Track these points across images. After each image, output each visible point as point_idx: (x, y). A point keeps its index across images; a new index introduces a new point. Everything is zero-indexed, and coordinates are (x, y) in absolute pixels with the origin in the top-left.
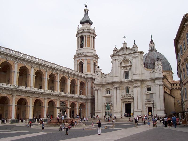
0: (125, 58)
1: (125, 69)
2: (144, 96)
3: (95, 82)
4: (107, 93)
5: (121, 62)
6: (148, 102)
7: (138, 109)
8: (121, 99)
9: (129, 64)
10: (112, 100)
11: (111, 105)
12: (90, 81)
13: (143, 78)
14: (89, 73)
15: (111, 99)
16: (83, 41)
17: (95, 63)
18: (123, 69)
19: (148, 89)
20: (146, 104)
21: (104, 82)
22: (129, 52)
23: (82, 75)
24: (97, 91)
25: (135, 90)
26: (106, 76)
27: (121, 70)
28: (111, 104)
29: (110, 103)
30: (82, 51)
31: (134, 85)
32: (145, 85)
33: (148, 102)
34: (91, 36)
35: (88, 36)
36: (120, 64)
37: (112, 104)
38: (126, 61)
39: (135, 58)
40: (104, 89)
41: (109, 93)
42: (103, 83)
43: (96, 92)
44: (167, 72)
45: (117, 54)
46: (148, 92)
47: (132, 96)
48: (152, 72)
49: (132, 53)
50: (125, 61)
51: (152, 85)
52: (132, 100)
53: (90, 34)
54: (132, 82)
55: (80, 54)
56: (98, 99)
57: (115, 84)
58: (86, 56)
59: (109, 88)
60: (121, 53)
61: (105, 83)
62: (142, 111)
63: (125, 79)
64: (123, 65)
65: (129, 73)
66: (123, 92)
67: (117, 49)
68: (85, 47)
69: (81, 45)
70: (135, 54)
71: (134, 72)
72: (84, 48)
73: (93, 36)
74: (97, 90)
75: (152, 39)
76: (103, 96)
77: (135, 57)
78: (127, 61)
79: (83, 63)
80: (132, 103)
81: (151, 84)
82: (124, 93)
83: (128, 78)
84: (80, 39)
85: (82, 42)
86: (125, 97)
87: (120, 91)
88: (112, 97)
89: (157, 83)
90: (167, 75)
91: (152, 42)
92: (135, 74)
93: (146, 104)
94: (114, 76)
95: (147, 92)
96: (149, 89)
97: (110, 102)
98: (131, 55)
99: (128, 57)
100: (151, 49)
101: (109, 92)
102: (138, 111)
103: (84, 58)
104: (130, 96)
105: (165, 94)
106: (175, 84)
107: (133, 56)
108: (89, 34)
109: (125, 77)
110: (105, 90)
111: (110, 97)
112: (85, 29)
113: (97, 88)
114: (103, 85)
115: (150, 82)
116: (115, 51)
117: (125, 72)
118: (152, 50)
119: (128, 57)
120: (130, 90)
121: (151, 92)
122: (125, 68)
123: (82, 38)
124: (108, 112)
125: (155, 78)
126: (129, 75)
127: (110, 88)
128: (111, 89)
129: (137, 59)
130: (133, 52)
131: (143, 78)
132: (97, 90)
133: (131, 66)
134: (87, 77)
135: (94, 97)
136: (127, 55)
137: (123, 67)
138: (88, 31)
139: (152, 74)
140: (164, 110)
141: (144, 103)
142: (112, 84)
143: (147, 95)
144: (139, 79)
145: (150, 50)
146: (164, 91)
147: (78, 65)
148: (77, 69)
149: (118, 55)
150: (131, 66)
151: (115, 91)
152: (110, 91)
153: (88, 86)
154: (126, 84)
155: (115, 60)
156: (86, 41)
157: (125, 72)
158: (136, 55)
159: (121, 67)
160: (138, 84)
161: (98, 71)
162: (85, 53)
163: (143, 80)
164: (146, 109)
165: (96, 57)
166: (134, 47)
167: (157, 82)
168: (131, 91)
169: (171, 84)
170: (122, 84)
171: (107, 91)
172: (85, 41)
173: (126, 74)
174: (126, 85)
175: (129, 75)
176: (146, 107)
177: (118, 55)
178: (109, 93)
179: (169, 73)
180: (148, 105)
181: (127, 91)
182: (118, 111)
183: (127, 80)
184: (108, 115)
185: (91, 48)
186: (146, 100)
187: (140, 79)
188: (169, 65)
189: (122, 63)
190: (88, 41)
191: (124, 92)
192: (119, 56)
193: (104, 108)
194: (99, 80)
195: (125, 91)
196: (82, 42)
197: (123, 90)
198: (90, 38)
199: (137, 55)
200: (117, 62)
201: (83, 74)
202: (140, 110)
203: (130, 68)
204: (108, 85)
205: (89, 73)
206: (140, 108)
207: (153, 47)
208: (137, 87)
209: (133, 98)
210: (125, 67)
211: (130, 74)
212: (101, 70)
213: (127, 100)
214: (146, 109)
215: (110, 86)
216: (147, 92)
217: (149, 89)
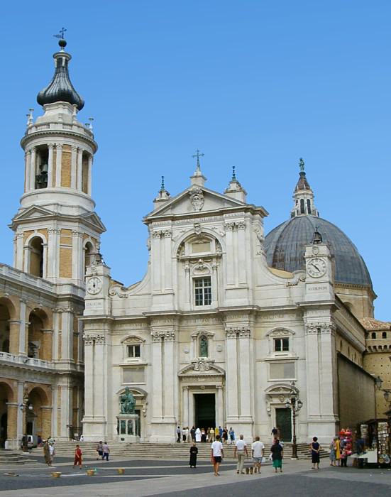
0: (197, 229)
1: (196, 269)
2: (264, 369)
3: (86, 313)
4: (131, 354)
5: (183, 244)
6: (278, 389)
7: (239, 414)
8: (180, 378)
9: (212, 250)
10: (147, 379)
11: (143, 398)
12: (69, 310)
13: (261, 303)
14: (65, 280)
15: (144, 376)
16: (47, 163)
17: (88, 246)
18: (187, 266)
19: (277, 342)
20: (270, 396)
21: (117, 313)
22: (210, 206)
23: (38, 284)
24: (94, 345)
25: (231, 343)
26: (127, 293)
27: (182, 273)
28: (143, 395)
29: (139, 389)
30: (43, 199)
31: (228, 325)
32: (269, 326)
33: (278, 389)
34: (78, 149)
35: (64, 146)
36: (180, 248)
37: (146, 394)
38: (201, 238)
39: (235, 230)
40: (117, 340)
41: (138, 355)
42: (114, 317)
43: (88, 349)
44: (355, 292)
45: (169, 213)
46: (278, 353)
47: (221, 366)
48: (293, 281)
49: (221, 213)
50: (195, 240)
51: (293, 329)
52: (218, 383)
53: (72, 140)
54: (221, 316)
55: (35, 210)
56: (93, 375)
57: (159, 323)
58: (58, 218)
59: (135, 337)
60: (181, 210)
61: (121, 317)
62: (253, 423)
63: (197, 304)
64: (189, 252)
65: (210, 285)
66: (186, 353)
67: (168, 194)
68: (54, 186)
69: (37, 178)
70: (233, 214)
71: (230, 279)
72: (49, 188)
73: (84, 147)
74: (94, 341)
75: (303, 174)
76: (115, 366)
77: (235, 227)
78: (204, 241)
79: (45, 242)
80: (220, 391)
81: (289, 323)
82: (192, 354)
83: (208, 302)
84: (36, 157)
85: (41, 167)
86: (193, 369)
87: (174, 347)
88: (147, 369)
89: (313, 321)
90: (352, 302)
91: (303, 183)
92: (233, 287)
93: (270, 396)
94: (156, 293)
95: (274, 355)
96: (282, 344)
97: (141, 387)
98: (220, 220)
99: (207, 226)
100: (299, 209)
101: (135, 351)
102: (241, 420)
103: (50, 225)
104: (211, 368)
105: (342, 363)
106: (381, 333)
107: (227, 221)
108: (70, 141)
109: (197, 298)
110: (122, 342)
111: (141, 368)
112: (55, 123)
113: (93, 334)
114: (113, 323)
115: (287, 317)
116: (162, 203)
118: (303, 211)
119: (207, 226)
120: (212, 346)
121: (289, 354)
122: (197, 266)
123: (43, 152)
124: (130, 422)
125: (305, 303)
126: (210, 291)
127: (139, 335)
128: (144, 341)
129: (241, 231)
130: (227, 207)
131: (261, 304)
132: (94, 341)
133: (219, 257)
134: (58, 295)
135: (83, 367)
136: (203, 219)
137: (191, 260)
138: (68, 129)
139: (294, 289)
140: (333, 419)
141: (262, 394)
142: (148, 320)
143: (273, 362)
144: (246, 307)
145: (294, 213)
146: (335, 355)
147: (27, 251)
148: (23, 263)
149: (173, 219)
150: (219, 257)
151: (157, 348)
152: (141, 347)
153: (60, 328)
154: (199, 322)
155: (162, 235)
156: (59, 166)
158: (239, 218)
159: (183, 261)
160: (243, 323)
161: (97, 274)
162: (51, 208)
163: (260, 308)
164: (270, 416)
165: (95, 223)
166: (232, 192)
167: (312, 318)
168: (215, 349)
169: (366, 333)
170: (184, 323)
171: (130, 348)
172: (54, 164)
173: (201, 285)
174: (199, 327)
175: (210, 289)
176: (269, 410)
177: (173, 219)
178: (138, 355)
179: (359, 292)
180: (276, 401)
181: (201, 347)
182: (166, 421)
183: (204, 307)
184: (129, 433)
185: (75, 191)
186: (270, 384)
187: (250, 306)
188: (360, 266)
189: (186, 245)
190: (66, 166)
191: (191, 354)
192: (176, 222)
193: (117, 408)
194: (99, 304)
195: (194, 347)
196: (44, 170)
197: (187, 345)
198: (74, 153)
199: (242, 220)
200: (167, 240)
201: (44, 281)
202: (249, 420)
203: (214, 264)
204: (134, 326)
205: (65, 280)
206: (246, 412)
207: (306, 201)
210: (196, 259)
211: (213, 288)
212: (110, 268)
213: (201, 382)
214: (270, 416)
215: (139, 327)
216: (274, 355)
217: (282, 344)
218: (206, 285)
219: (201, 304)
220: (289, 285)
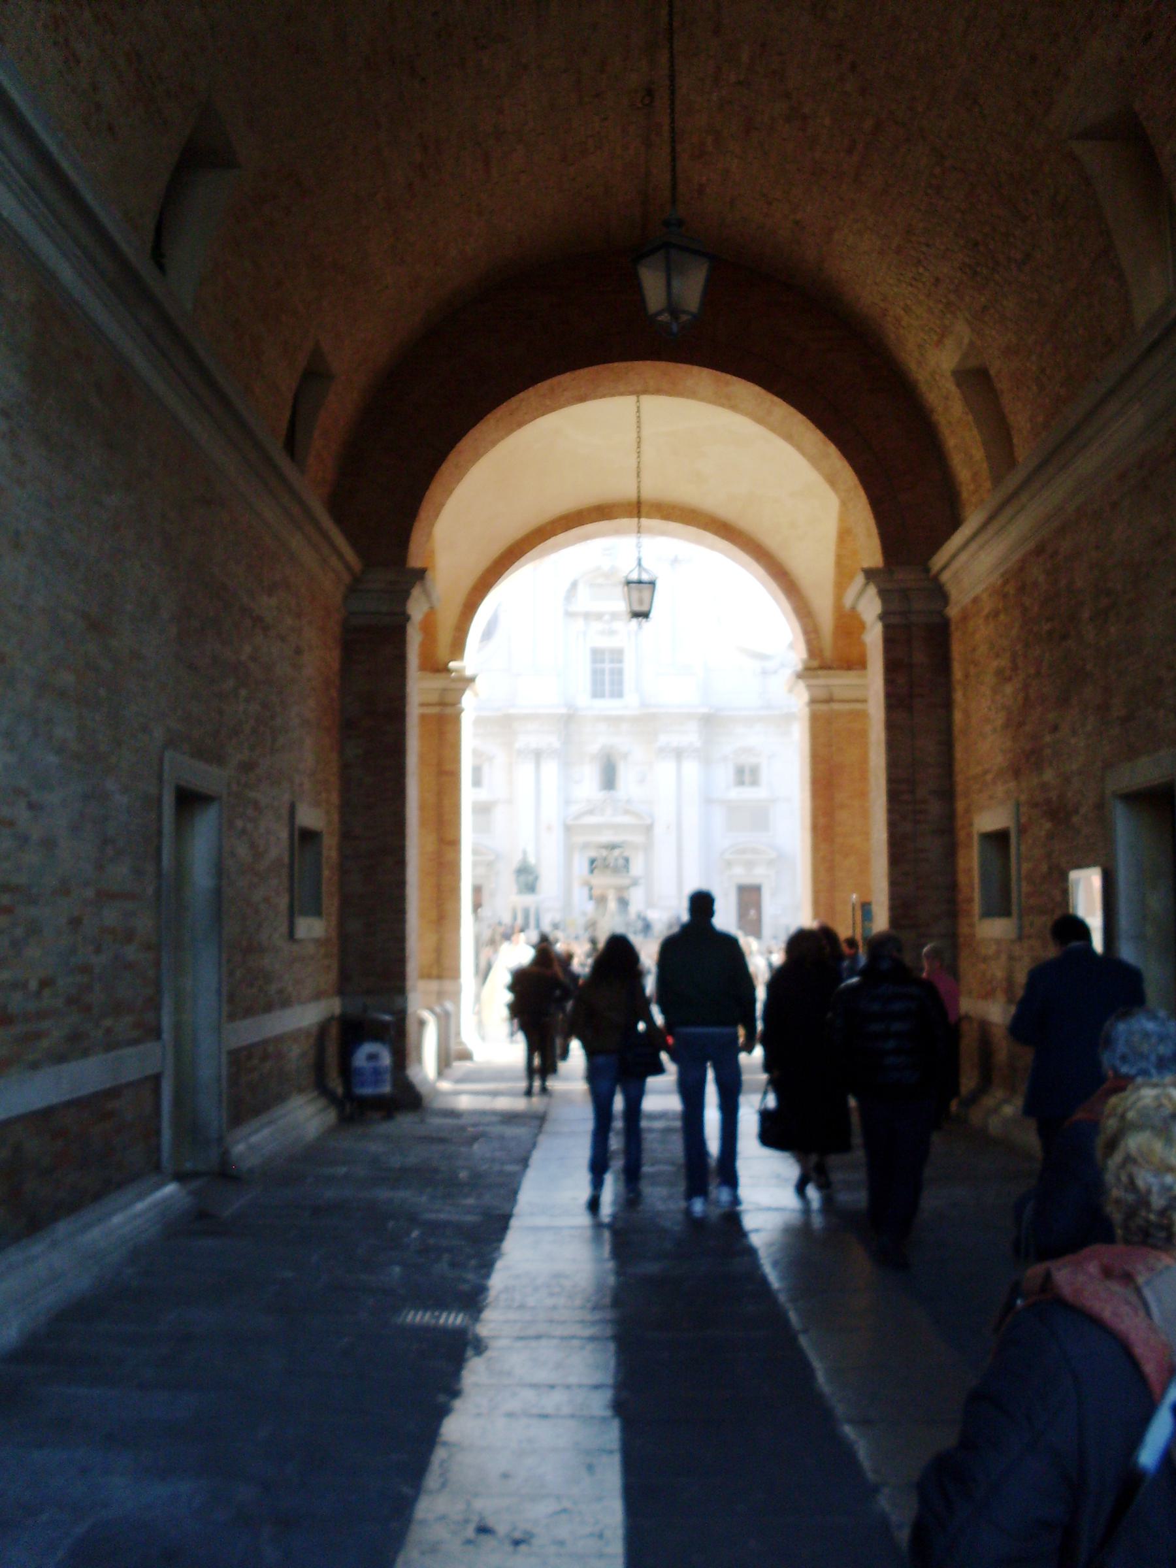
5: (574, 585)
8: (568, 829)
20: (729, 864)
25: (666, 769)
31: (663, 739)
65: (620, 661)
86: (591, 812)
95: (735, 793)
104: (627, 812)
117: (597, 655)
121: (758, 794)
137: (587, 616)
151: (526, 770)
157: (597, 655)
173: (603, 661)
175: (620, 672)
208: (679, 754)
209: (648, 822)
210: (599, 616)
216: (735, 793)
218: (612, 661)
219: (602, 696)
220: (765, 673)
